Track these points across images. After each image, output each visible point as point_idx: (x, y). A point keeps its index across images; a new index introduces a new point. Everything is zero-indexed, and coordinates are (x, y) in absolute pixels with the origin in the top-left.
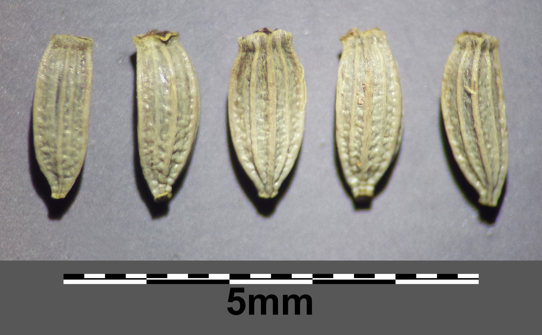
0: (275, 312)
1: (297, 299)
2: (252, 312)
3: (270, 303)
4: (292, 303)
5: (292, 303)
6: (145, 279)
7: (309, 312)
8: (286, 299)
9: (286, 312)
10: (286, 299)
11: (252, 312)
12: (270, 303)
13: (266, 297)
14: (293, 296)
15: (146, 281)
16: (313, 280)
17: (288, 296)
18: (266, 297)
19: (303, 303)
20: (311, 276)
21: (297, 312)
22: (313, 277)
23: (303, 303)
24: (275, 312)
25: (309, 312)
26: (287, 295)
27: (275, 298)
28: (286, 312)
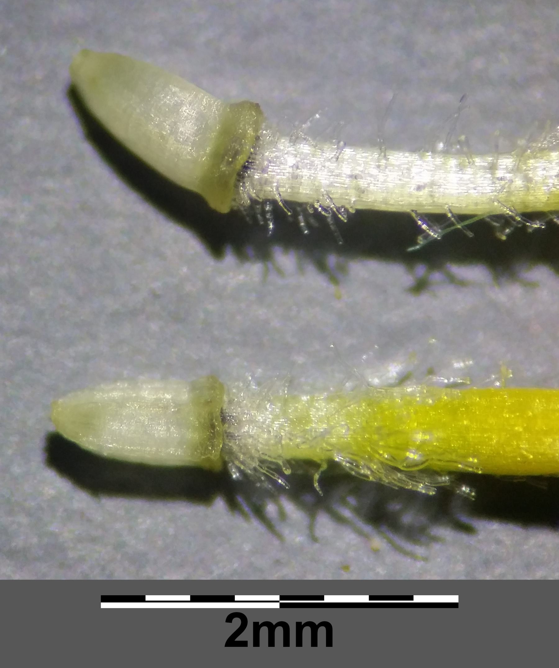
0: (286, 643)
3: (279, 632)
5: (307, 632)
6: (278, 602)
8: (300, 627)
9: (299, 643)
12: (279, 632)
15: (278, 604)
16: (280, 603)
17: (303, 624)
20: (277, 598)
21: (314, 643)
22: (281, 599)
24: (286, 643)
27: (285, 626)
28: (299, 643)
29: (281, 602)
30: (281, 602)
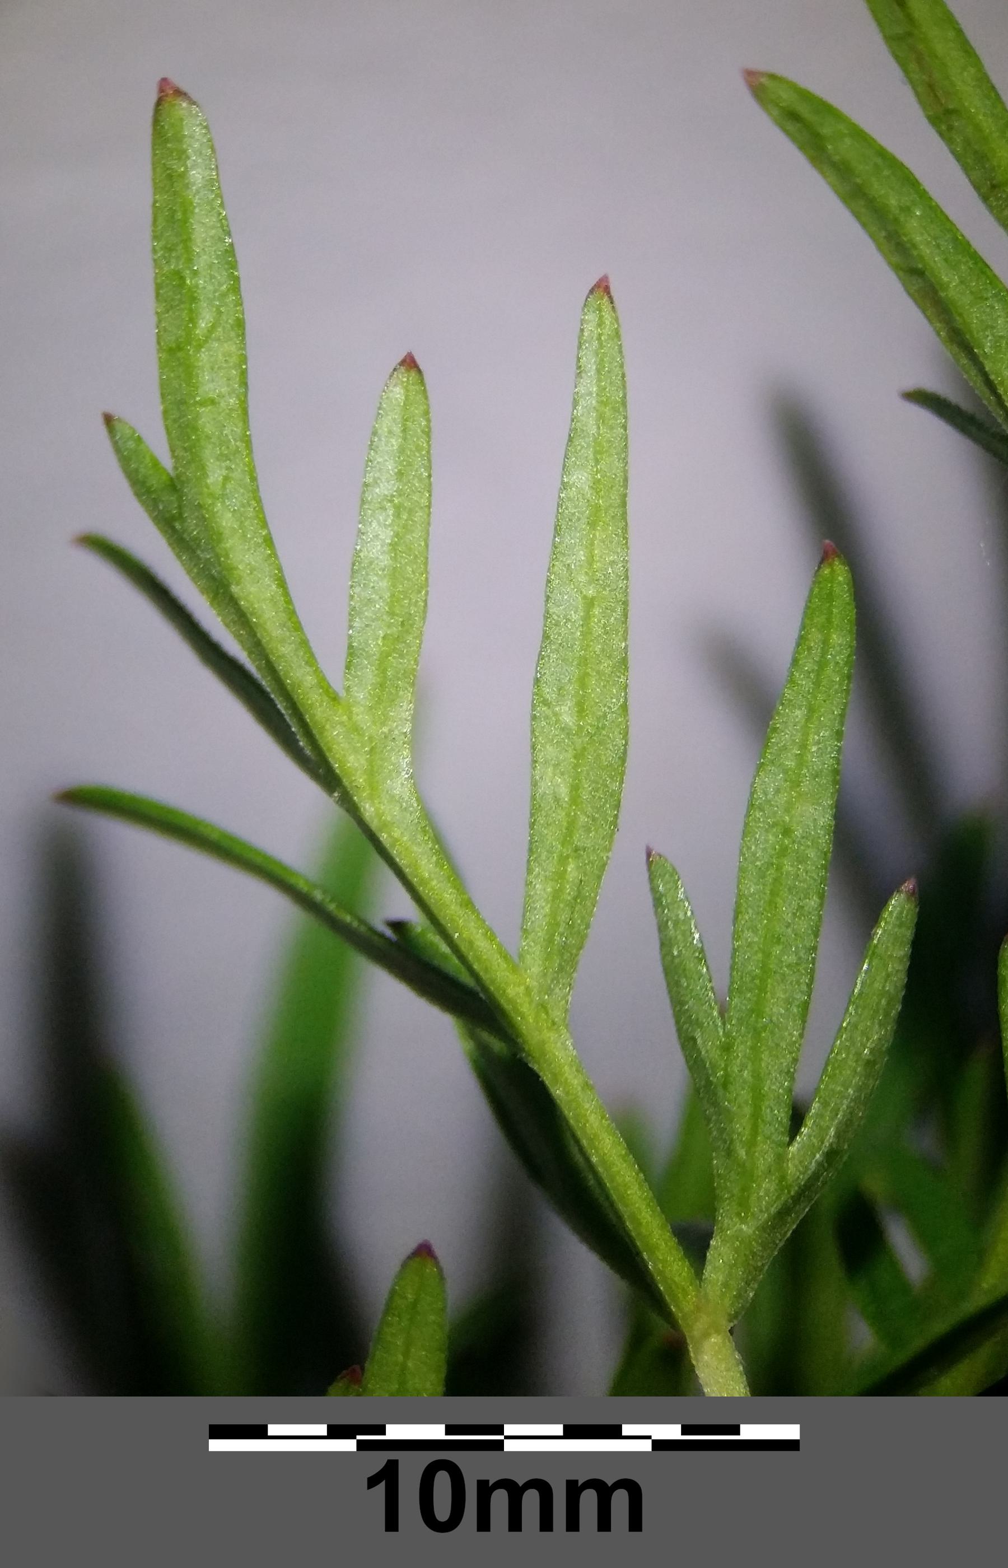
1: (604, 1492)
2: (484, 1524)
3: (531, 1500)
4: (589, 1500)
5: (589, 1500)
7: (635, 1523)
8: (574, 1490)
10: (574, 1490)
11: (484, 1524)
12: (531, 1500)
13: (520, 1485)
14: (594, 1484)
17: (579, 1485)
18: (520, 1485)
19: (620, 1500)
21: (604, 1524)
23: (620, 1500)
24: (546, 1524)
25: (635, 1523)
26: (577, 1481)
27: (544, 1488)
28: (573, 1524)
29: (501, 1437)
30: (501, 1437)
